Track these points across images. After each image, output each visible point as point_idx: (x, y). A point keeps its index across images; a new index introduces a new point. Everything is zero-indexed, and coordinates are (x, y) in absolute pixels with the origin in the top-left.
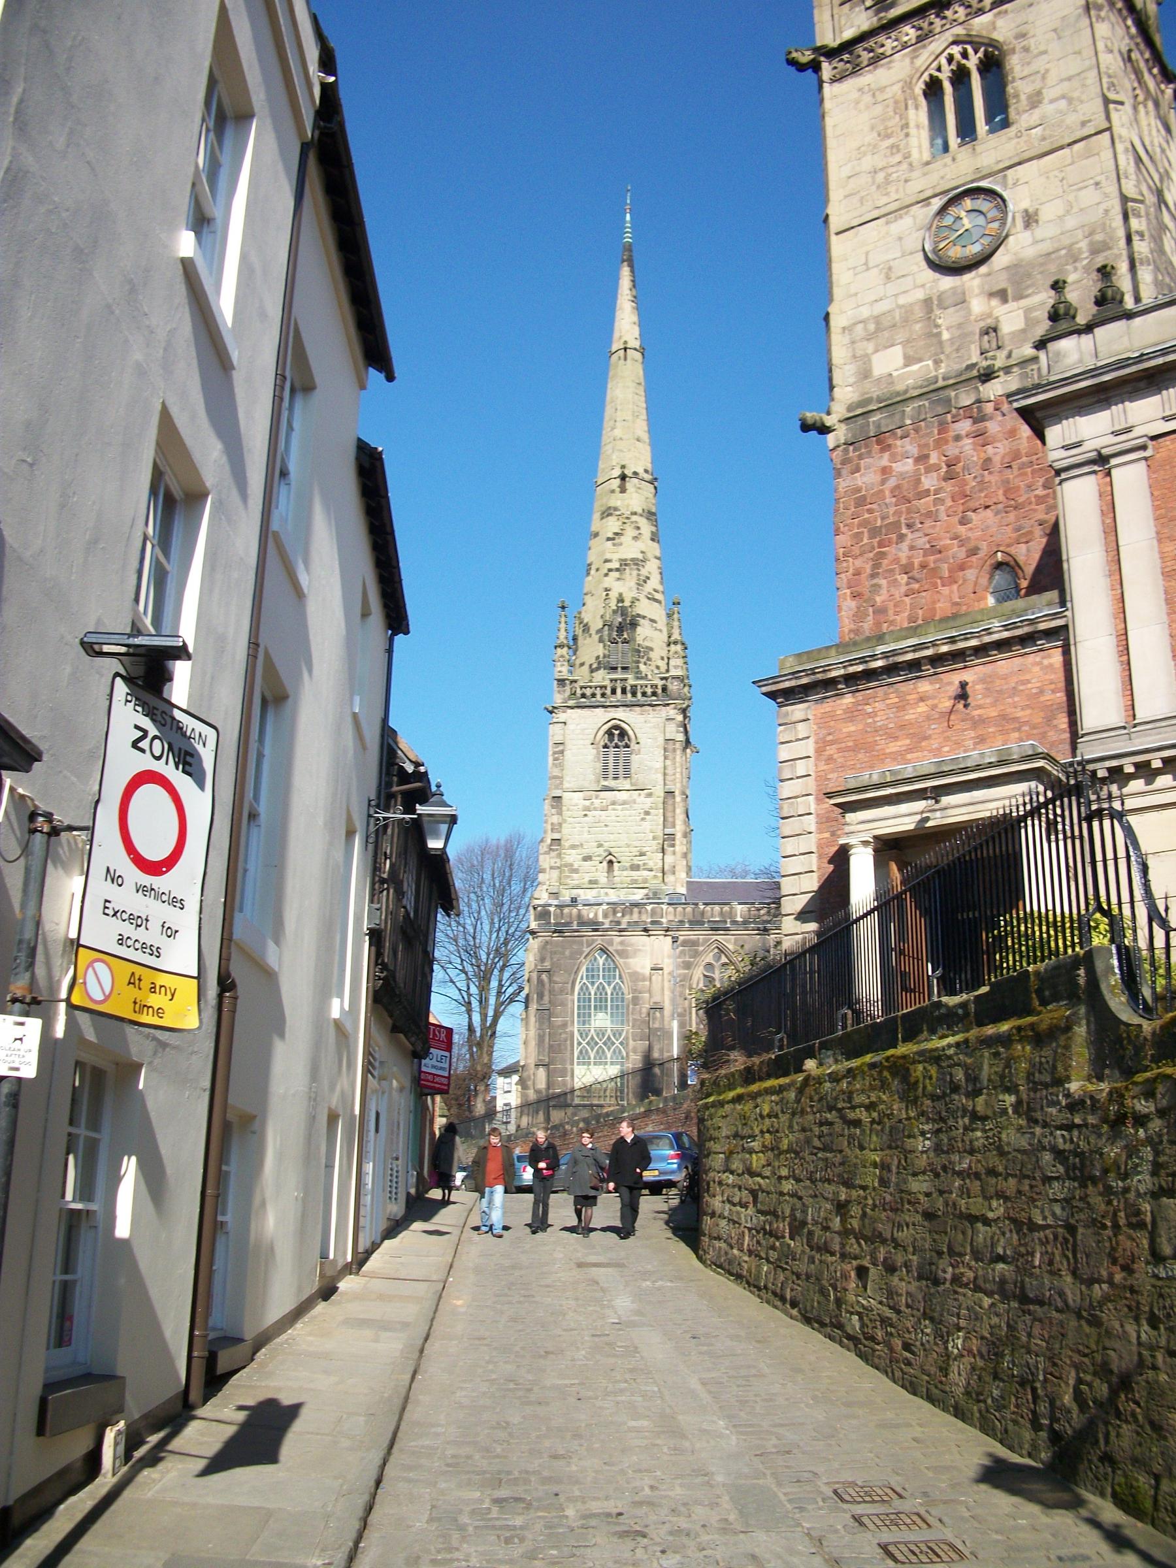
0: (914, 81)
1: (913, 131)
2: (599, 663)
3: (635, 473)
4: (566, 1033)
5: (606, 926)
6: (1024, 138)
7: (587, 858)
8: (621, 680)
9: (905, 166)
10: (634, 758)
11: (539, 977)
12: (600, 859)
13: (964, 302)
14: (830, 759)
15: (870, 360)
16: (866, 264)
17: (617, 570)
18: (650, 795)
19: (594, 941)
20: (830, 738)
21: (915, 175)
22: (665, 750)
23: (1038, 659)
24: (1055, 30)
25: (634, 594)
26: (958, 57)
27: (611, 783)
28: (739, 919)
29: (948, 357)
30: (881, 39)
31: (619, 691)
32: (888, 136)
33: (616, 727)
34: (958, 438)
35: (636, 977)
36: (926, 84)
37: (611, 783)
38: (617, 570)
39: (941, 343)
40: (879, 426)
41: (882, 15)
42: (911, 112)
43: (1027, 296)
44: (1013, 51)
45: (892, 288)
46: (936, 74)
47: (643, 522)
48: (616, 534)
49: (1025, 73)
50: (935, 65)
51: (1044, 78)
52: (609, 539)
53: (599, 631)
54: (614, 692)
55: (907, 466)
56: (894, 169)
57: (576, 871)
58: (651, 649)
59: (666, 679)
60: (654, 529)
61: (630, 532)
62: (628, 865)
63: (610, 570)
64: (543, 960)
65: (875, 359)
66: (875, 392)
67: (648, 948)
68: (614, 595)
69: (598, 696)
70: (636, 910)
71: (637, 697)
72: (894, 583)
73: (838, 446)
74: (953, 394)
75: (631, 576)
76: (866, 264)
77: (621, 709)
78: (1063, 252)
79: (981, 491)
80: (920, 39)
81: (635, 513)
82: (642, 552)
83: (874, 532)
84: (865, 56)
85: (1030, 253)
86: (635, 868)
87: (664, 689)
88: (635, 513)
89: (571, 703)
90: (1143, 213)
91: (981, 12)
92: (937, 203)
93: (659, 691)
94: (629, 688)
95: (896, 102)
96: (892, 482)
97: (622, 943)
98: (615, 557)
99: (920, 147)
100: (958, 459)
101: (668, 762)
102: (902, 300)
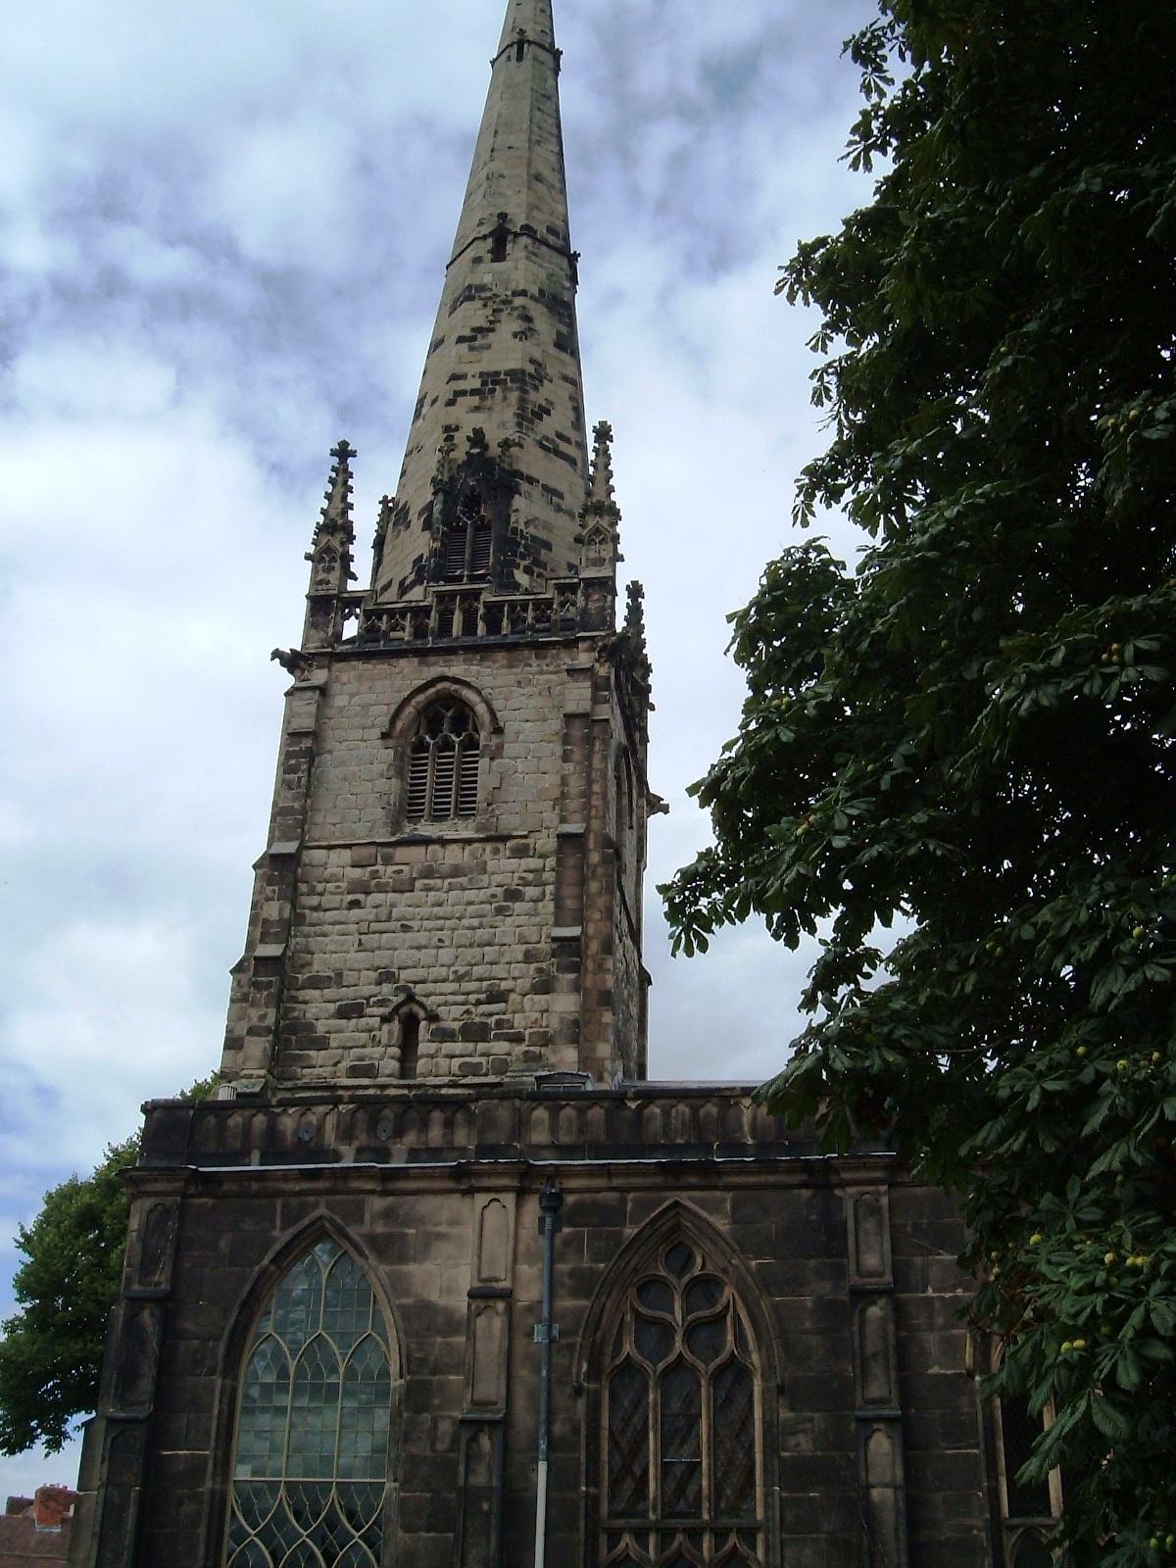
5: (347, 1163)
8: (465, 594)
10: (483, 763)
18: (521, 852)
19: (304, 1209)
22: (566, 740)
25: (511, 433)
27: (426, 829)
35: (422, 1320)
37: (426, 829)
38: (474, 392)
47: (537, 311)
48: (478, 330)
52: (461, 340)
57: (322, 1044)
58: (548, 546)
60: (564, 330)
62: (456, 1025)
63: (463, 393)
67: (470, 1232)
70: (437, 1116)
81: (524, 293)
82: (532, 361)
86: (474, 1032)
88: (524, 293)
97: (388, 1214)
101: (570, 767)
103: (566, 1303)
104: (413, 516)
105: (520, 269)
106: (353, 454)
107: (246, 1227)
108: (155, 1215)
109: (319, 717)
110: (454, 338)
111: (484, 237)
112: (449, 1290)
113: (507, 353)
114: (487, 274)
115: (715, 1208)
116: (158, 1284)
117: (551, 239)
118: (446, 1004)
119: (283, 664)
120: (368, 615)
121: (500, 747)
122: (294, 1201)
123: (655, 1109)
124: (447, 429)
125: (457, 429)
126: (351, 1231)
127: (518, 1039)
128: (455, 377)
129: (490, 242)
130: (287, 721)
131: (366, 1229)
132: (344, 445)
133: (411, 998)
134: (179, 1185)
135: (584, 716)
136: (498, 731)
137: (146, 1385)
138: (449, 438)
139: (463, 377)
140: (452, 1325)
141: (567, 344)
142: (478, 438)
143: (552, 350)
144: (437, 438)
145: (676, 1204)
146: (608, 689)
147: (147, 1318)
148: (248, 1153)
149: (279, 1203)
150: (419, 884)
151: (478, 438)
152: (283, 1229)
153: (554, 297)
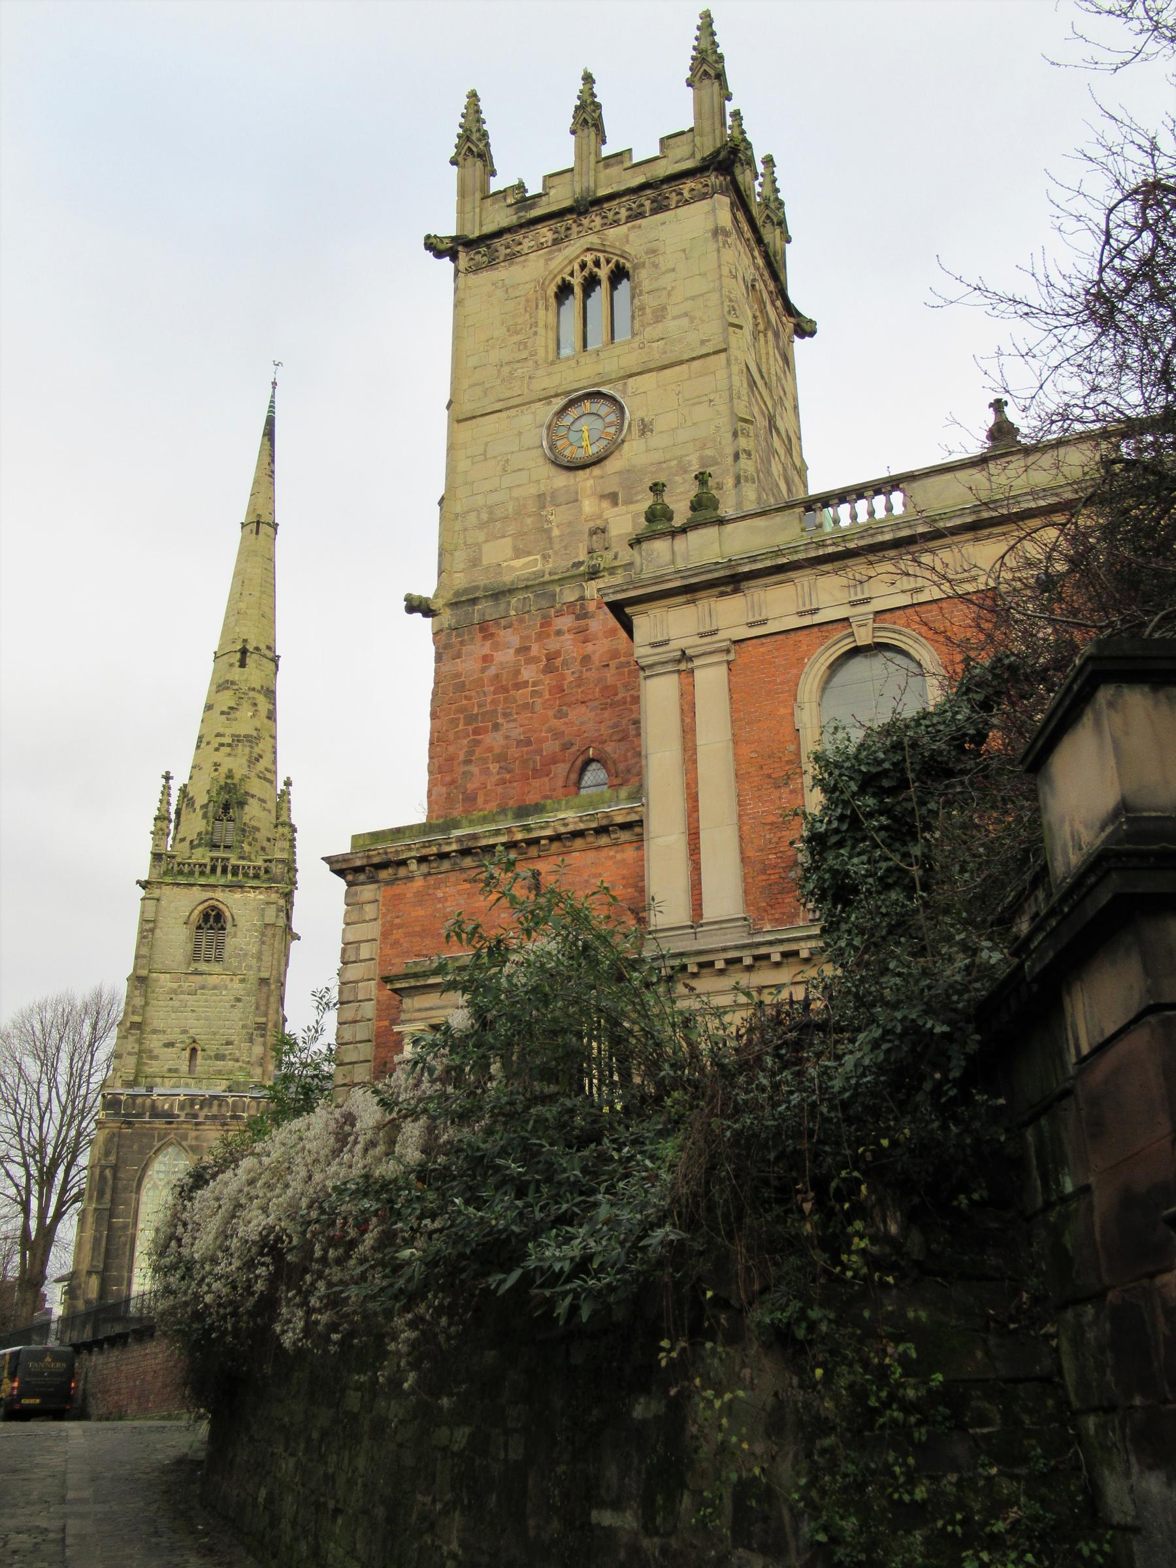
0: (547, 282)
1: (541, 331)
2: (201, 839)
3: (257, 649)
4: (126, 1236)
5: (182, 1119)
6: (646, 350)
7: (170, 1045)
8: (223, 859)
9: (531, 363)
10: (227, 940)
11: (102, 1173)
12: (183, 1046)
13: (577, 500)
14: (396, 943)
15: (480, 549)
16: (484, 454)
17: (229, 745)
19: (166, 1135)
20: (397, 921)
21: (540, 373)
22: (263, 934)
23: (612, 853)
24: (684, 251)
25: (245, 771)
26: (590, 264)
29: (556, 553)
30: (518, 237)
31: (219, 869)
32: (517, 333)
33: (213, 908)
34: (559, 633)
36: (559, 287)
37: (203, 967)
38: (229, 745)
39: (550, 538)
40: (484, 615)
41: (522, 214)
42: (541, 312)
43: (637, 501)
44: (643, 265)
45: (507, 481)
46: (568, 278)
47: (261, 699)
49: (652, 288)
50: (568, 270)
51: (669, 295)
52: (223, 713)
53: (205, 806)
54: (213, 870)
55: (506, 656)
56: (519, 365)
57: (156, 1058)
58: (258, 829)
59: (270, 861)
60: (271, 707)
62: (212, 1054)
63: (222, 745)
64: (107, 1153)
65: (486, 547)
66: (482, 580)
68: (223, 770)
69: (197, 874)
70: (216, 1103)
71: (238, 878)
72: (486, 771)
73: (441, 630)
74: (558, 589)
75: (243, 750)
76: (484, 454)
77: (220, 889)
78: (674, 463)
79: (579, 686)
80: (556, 242)
81: (254, 689)
83: (470, 719)
84: (503, 251)
85: (641, 460)
86: (219, 1057)
87: (267, 871)
88: (254, 689)
89: (168, 880)
90: (751, 434)
91: (616, 223)
92: (559, 403)
93: (262, 873)
94: (230, 868)
95: (527, 301)
96: (492, 671)
97: (197, 1138)
98: (228, 732)
99: (546, 347)
100: (557, 654)
102: (516, 493)
105: (253, 675)
106: (172, 778)
109: (156, 912)
113: (245, 723)
114: (236, 674)
121: (235, 933)
124: (216, 764)
126: (184, 1143)
127: (237, 1060)
128: (218, 735)
129: (238, 655)
130: (143, 912)
132: (168, 773)
137: (108, 1196)
138: (216, 770)
141: (272, 716)
142: (230, 775)
143: (266, 721)
144: (208, 767)
147: (108, 1172)
151: (230, 775)
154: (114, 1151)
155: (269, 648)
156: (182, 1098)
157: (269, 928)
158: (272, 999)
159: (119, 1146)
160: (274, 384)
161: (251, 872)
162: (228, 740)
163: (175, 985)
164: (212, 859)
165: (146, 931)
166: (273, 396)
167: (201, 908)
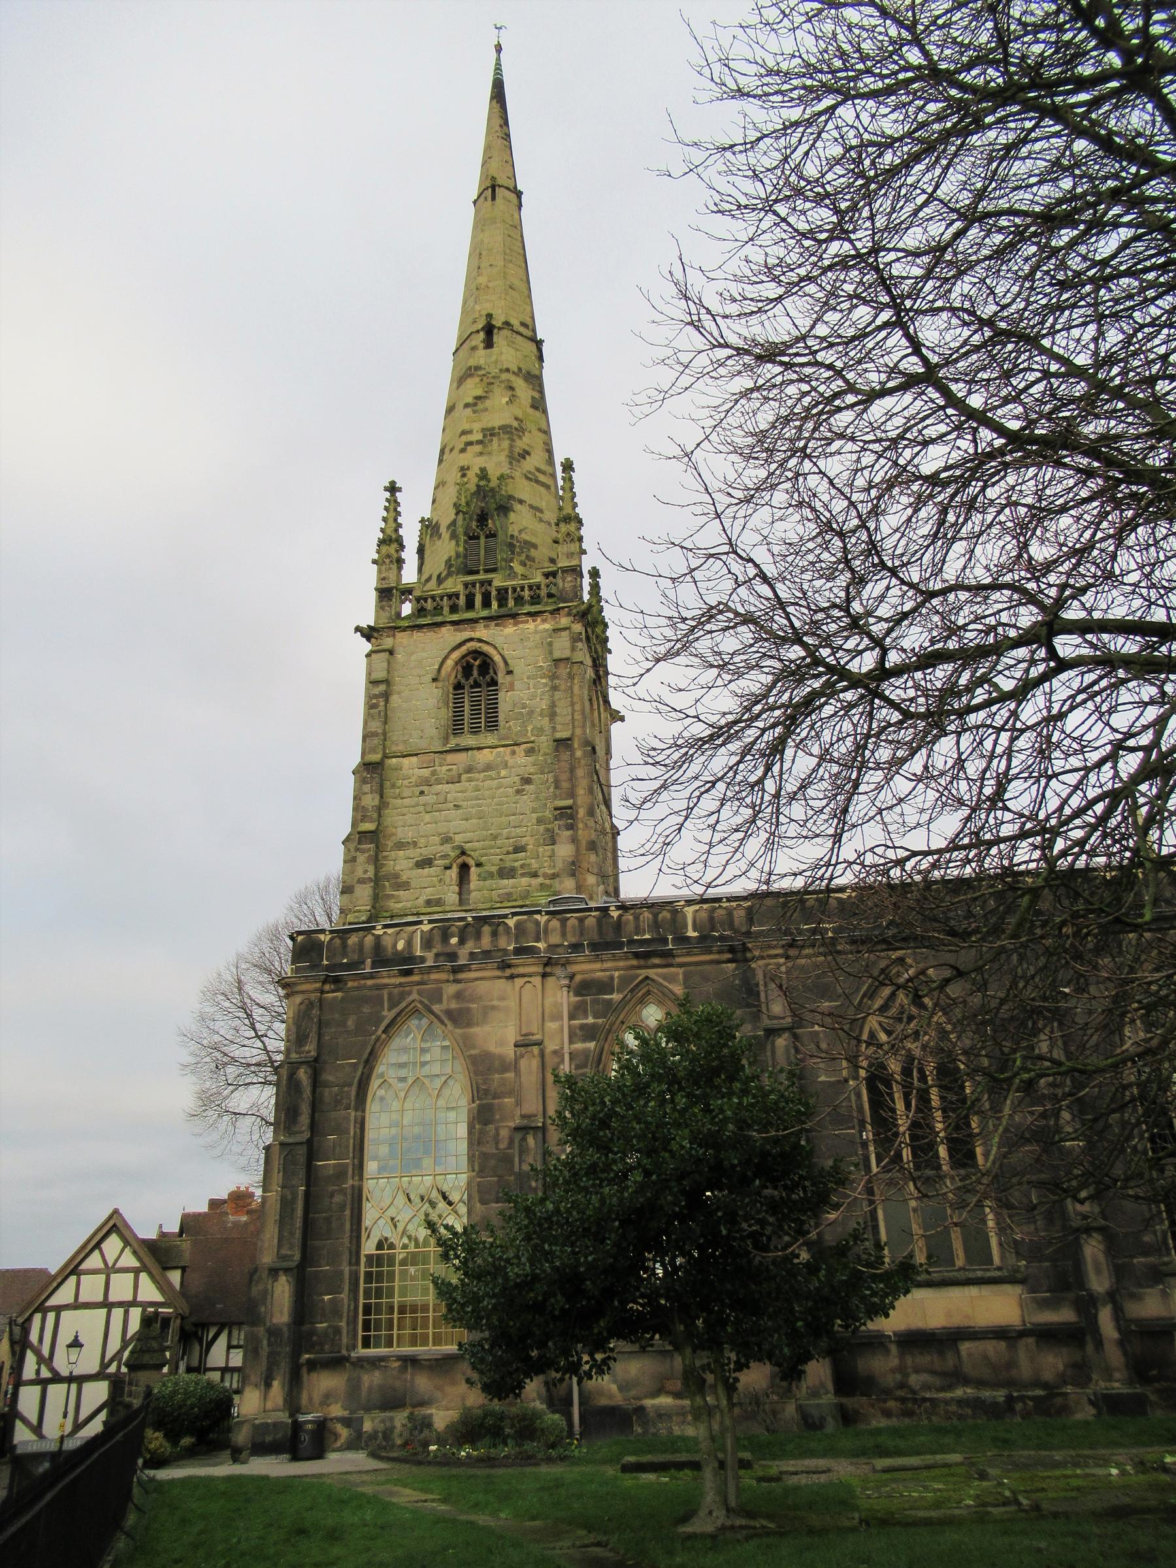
3: (507, 323)
4: (343, 1191)
5: (429, 963)
7: (425, 863)
8: (482, 583)
10: (501, 695)
12: (446, 862)
19: (402, 996)
22: (554, 677)
25: (506, 470)
28: (691, 933)
31: (478, 599)
33: (477, 653)
37: (468, 740)
38: (479, 442)
47: (519, 383)
48: (478, 398)
52: (467, 406)
57: (405, 886)
58: (535, 546)
60: (536, 395)
61: (500, 398)
62: (494, 869)
63: (470, 443)
67: (512, 1003)
68: (472, 475)
69: (446, 610)
70: (486, 930)
75: (500, 448)
77: (482, 624)
81: (508, 370)
82: (516, 419)
86: (506, 873)
88: (508, 370)
94: (494, 593)
97: (458, 996)
98: (476, 427)
103: (579, 1046)
104: (443, 529)
106: (400, 490)
107: (365, 1010)
108: (303, 1007)
110: (461, 405)
111: (478, 332)
112: (502, 1043)
113: (499, 411)
114: (482, 357)
115: (671, 979)
116: (309, 1052)
117: (522, 330)
118: (486, 855)
119: (363, 635)
120: (418, 600)
122: (396, 991)
123: (629, 917)
125: (468, 468)
126: (436, 1008)
127: (535, 875)
128: (464, 433)
129: (482, 335)
130: (369, 674)
131: (444, 1006)
132: (393, 483)
133: (463, 853)
134: (318, 985)
135: (567, 659)
136: (510, 672)
137: (304, 1120)
138: (464, 475)
139: (470, 432)
140: (505, 1068)
141: (539, 405)
142: (483, 475)
143: (531, 411)
144: (454, 476)
145: (647, 978)
146: (581, 640)
147: (303, 1075)
148: (363, 962)
149: (385, 993)
150: (464, 777)
151: (483, 475)
152: (389, 1010)
153: (528, 373)
154: (313, 1036)
155: (523, 324)
156: (426, 927)
157: (562, 665)
158: (580, 772)
159: (321, 1025)
160: (499, 49)
161: (526, 594)
162: (478, 436)
163: (426, 772)
164: (466, 585)
165: (375, 697)
166: (498, 59)
167: (456, 655)
